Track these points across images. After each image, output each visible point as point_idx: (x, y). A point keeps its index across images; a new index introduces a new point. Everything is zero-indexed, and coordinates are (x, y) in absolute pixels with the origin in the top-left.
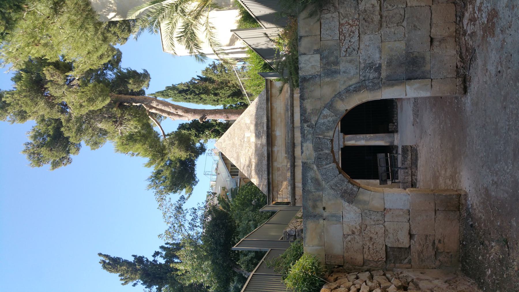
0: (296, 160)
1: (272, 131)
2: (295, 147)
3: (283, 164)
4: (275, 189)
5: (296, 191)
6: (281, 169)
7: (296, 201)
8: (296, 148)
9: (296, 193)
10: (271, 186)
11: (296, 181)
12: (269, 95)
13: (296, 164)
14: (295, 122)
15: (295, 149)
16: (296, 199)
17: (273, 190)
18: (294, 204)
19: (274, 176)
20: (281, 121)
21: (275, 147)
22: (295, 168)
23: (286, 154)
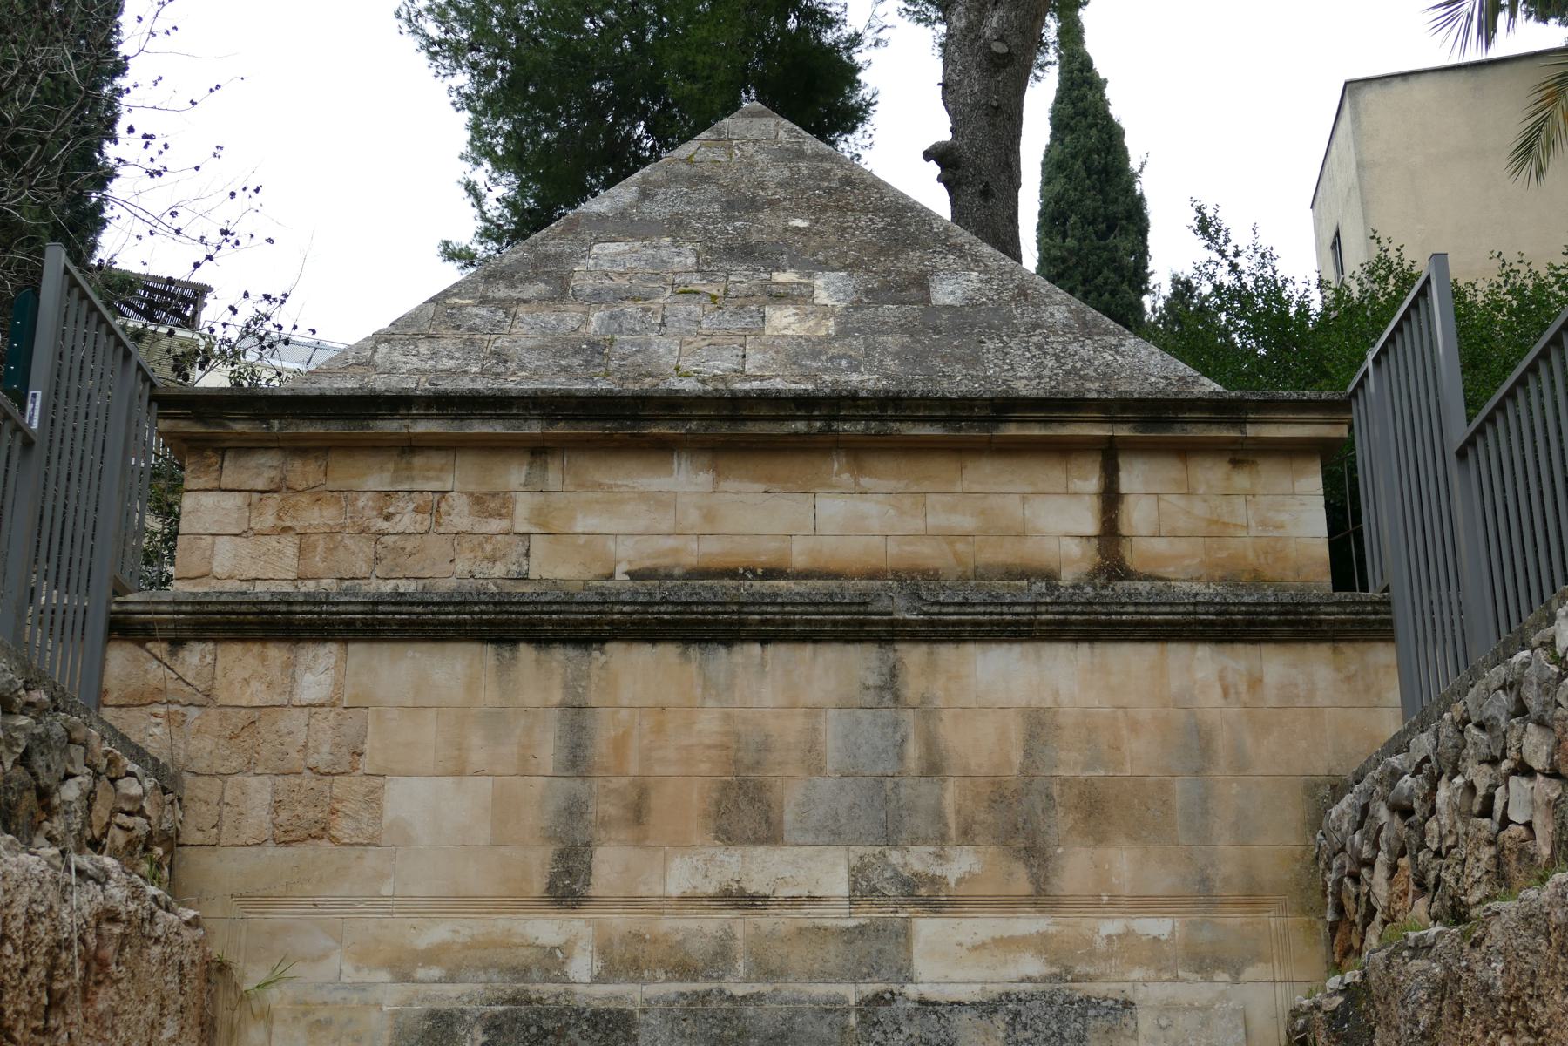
0: (560, 656)
1: (858, 450)
2: (694, 651)
3: (538, 544)
4: (303, 472)
5: (256, 648)
6: (495, 525)
7: (160, 649)
8: (683, 654)
9: (237, 649)
10: (335, 428)
11: (359, 652)
12: (1197, 432)
13: (526, 652)
14: (946, 652)
15: (668, 653)
16: (177, 643)
17: (299, 449)
18: (124, 629)
19: (437, 460)
20: (949, 536)
21: (704, 479)
22: (490, 648)
23: (633, 575)
